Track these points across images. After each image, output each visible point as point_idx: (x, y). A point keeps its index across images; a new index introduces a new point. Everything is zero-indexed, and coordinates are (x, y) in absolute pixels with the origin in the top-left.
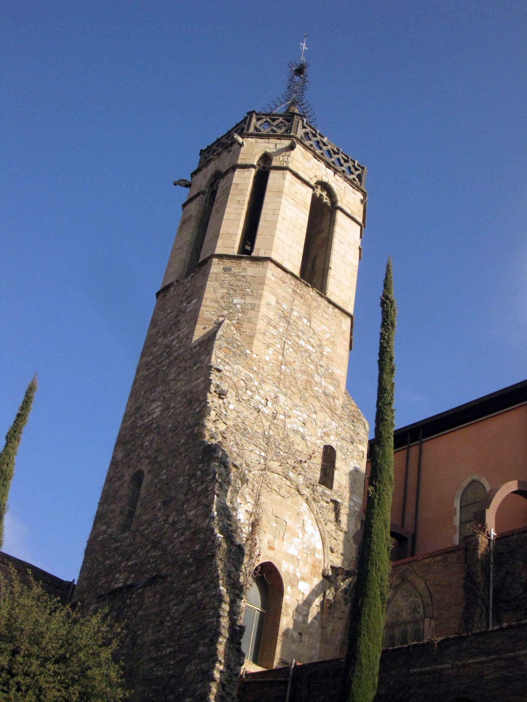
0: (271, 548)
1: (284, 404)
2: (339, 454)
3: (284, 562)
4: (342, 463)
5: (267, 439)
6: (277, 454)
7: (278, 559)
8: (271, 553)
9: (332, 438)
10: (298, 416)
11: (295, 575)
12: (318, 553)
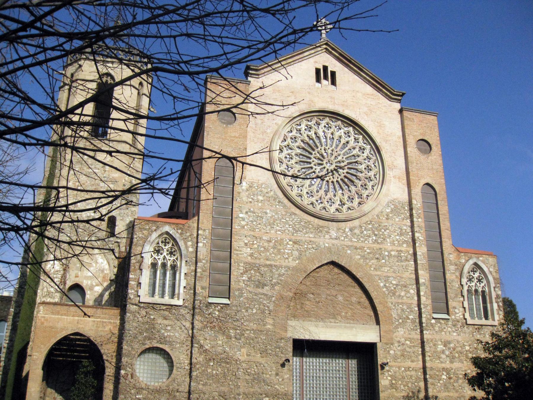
0: (77, 277)
2: (117, 218)
3: (85, 281)
4: (121, 222)
7: (81, 280)
8: (77, 279)
11: (92, 285)
12: (106, 270)
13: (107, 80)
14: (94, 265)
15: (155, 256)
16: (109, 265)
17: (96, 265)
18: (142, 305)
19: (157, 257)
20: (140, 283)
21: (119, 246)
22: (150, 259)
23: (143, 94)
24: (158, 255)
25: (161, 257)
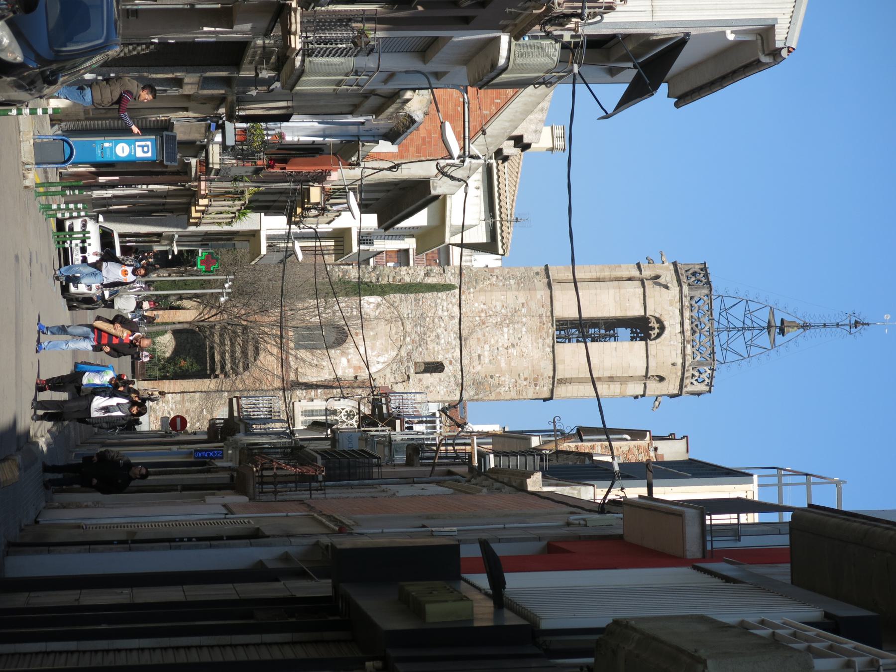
1: (452, 324)
4: (438, 379)
5: (423, 316)
6: (416, 325)
9: (451, 368)
10: (451, 337)
13: (654, 329)
14: (374, 354)
15: (344, 412)
16: (377, 372)
17: (374, 356)
18: (291, 405)
19: (342, 414)
20: (313, 401)
21: (404, 381)
22: (340, 408)
23: (645, 384)
24: (344, 415)
25: (344, 418)
